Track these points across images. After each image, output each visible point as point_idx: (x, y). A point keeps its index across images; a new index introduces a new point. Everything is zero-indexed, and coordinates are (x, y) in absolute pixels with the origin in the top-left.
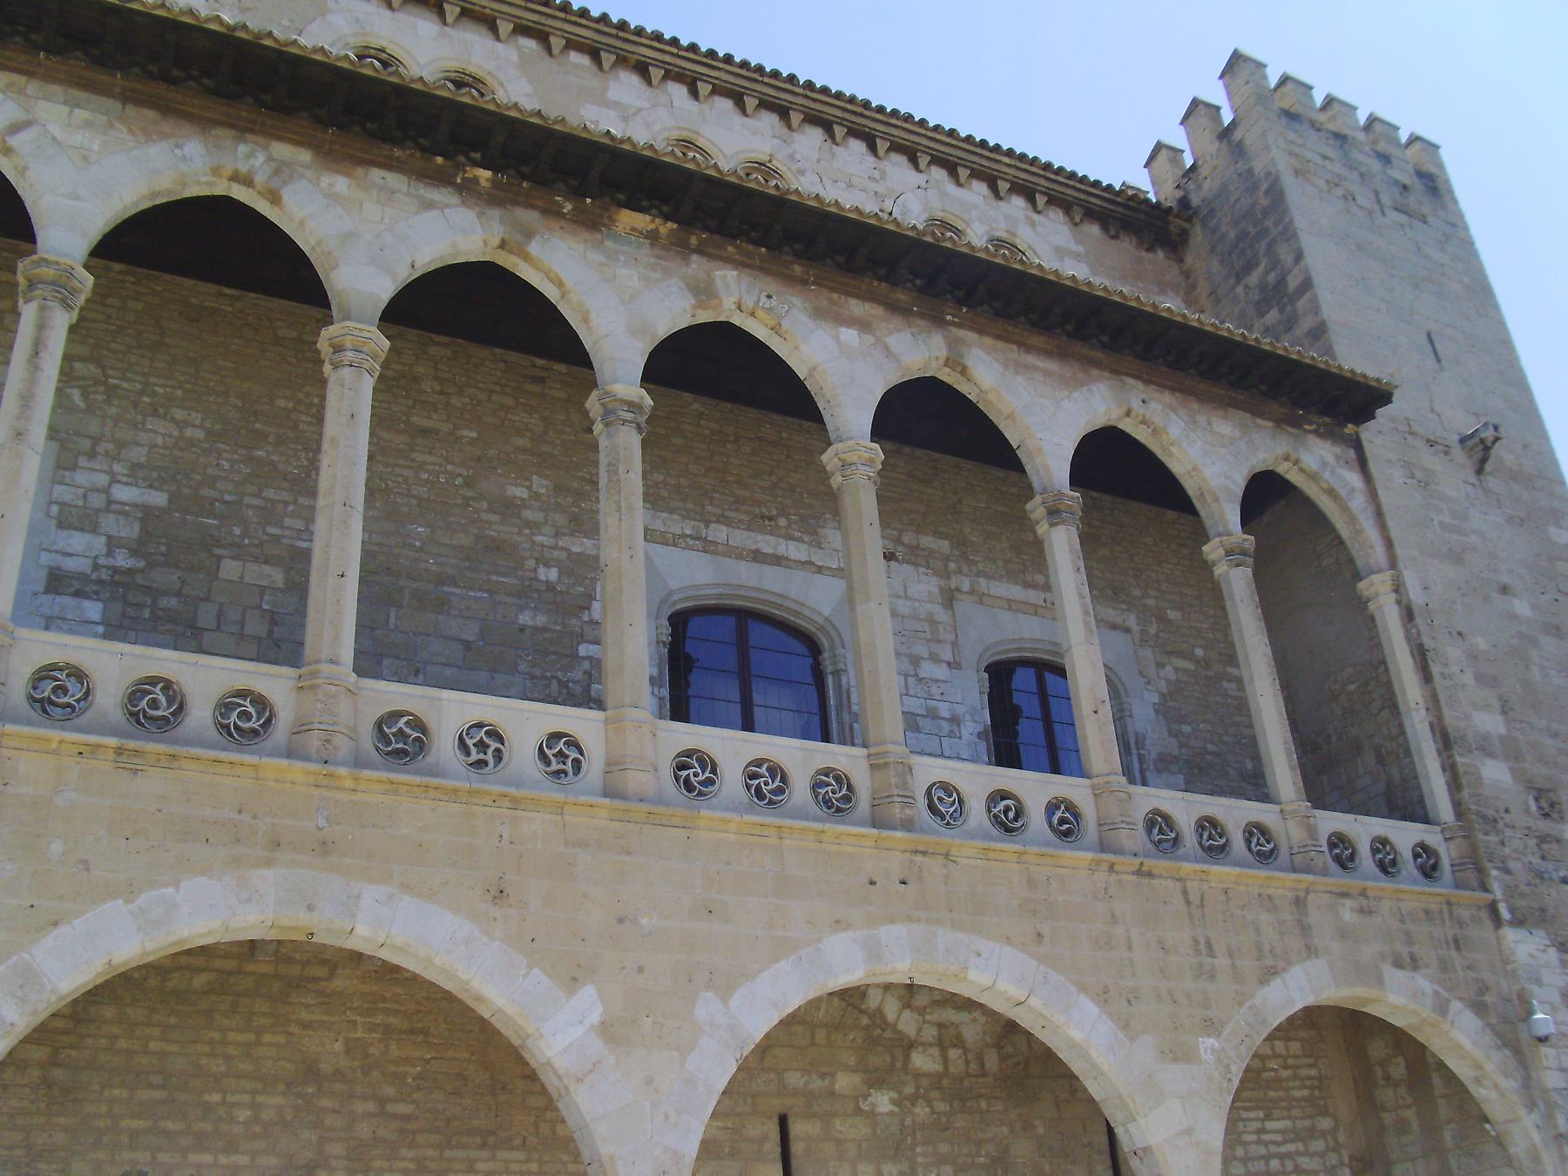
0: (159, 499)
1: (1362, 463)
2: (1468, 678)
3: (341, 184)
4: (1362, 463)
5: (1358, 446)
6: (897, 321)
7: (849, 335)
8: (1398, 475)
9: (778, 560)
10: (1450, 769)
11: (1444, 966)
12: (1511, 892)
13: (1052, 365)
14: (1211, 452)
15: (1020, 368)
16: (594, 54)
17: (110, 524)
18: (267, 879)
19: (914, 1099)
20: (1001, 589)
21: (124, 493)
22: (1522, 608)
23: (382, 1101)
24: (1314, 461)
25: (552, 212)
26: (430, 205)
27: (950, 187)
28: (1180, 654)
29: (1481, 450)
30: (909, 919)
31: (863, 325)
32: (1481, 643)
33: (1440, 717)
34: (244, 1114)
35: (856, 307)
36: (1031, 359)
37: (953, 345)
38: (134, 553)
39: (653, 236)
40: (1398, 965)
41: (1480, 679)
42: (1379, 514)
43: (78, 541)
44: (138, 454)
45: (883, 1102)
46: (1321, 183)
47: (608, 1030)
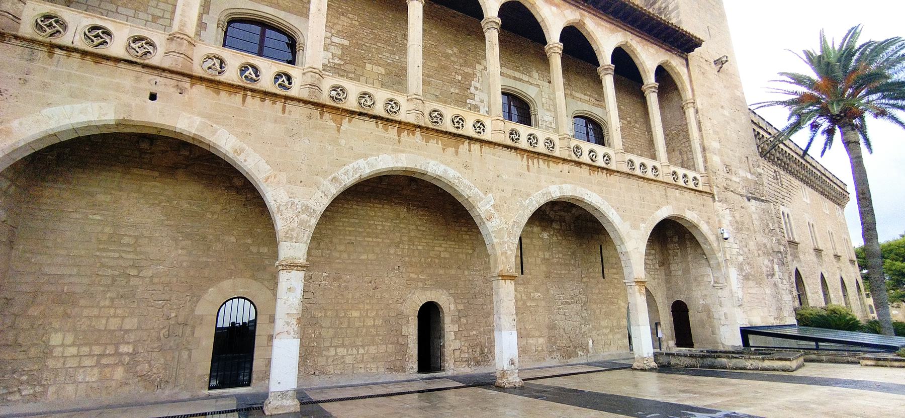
0: (346, 43)
1: (687, 65)
2: (711, 132)
4: (687, 65)
5: (687, 60)
6: (567, 5)
7: (554, 9)
8: (697, 70)
9: (520, 80)
10: (705, 158)
13: (608, 25)
14: (649, 57)
15: (598, 24)
18: (403, 156)
19: (553, 235)
20: (578, 95)
22: (726, 113)
23: (417, 226)
24: (675, 63)
29: (720, 63)
30: (571, 183)
33: (703, 142)
34: (380, 228)
38: (340, 59)
41: (714, 131)
42: (691, 81)
44: (339, 28)
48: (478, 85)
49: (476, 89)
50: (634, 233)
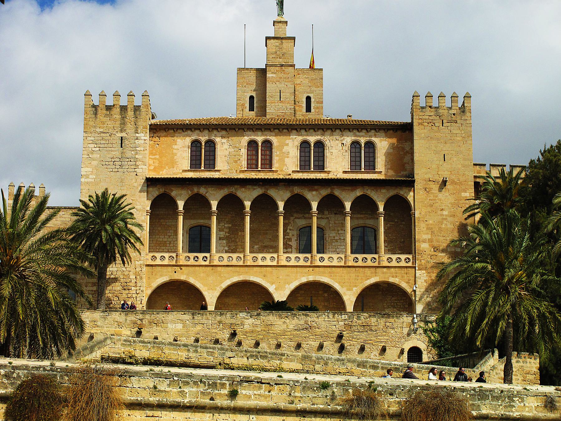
0: (230, 225)
3: (243, 189)
7: (314, 193)
8: (422, 192)
11: (402, 277)
12: (420, 265)
15: (344, 190)
16: (287, 129)
17: (225, 230)
21: (226, 226)
25: (270, 185)
26: (254, 189)
27: (358, 133)
28: (392, 221)
29: (444, 183)
31: (316, 190)
32: (431, 222)
35: (316, 187)
36: (346, 188)
37: (332, 189)
39: (285, 185)
40: (393, 277)
41: (427, 229)
43: (222, 233)
44: (227, 220)
45: (326, 295)
46: (426, 124)
47: (275, 289)
48: (291, 228)
49: (290, 230)
50: (349, 293)
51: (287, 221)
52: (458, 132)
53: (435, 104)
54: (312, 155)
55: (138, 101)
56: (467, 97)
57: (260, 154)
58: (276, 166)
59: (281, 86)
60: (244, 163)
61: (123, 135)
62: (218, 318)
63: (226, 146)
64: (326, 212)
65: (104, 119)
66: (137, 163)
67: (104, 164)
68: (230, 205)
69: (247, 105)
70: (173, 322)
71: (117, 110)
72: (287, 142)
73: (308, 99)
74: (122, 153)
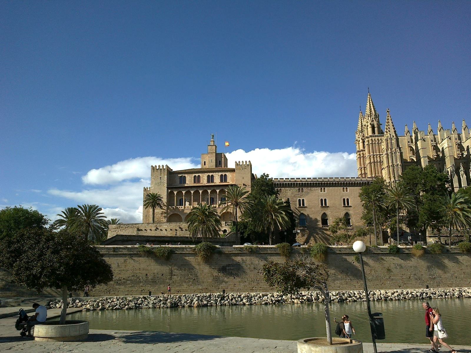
51: (204, 197)
52: (247, 171)
53: (241, 164)
54: (211, 179)
55: (165, 168)
56: (249, 161)
57: (197, 179)
58: (201, 182)
59: (212, 158)
60: (193, 181)
61: (161, 176)
62: (176, 224)
63: (189, 177)
64: (214, 194)
65: (156, 172)
66: (165, 183)
67: (156, 184)
68: (188, 193)
69: (204, 164)
70: (164, 225)
71: (159, 170)
72: (204, 175)
73: (220, 161)
74: (161, 181)
